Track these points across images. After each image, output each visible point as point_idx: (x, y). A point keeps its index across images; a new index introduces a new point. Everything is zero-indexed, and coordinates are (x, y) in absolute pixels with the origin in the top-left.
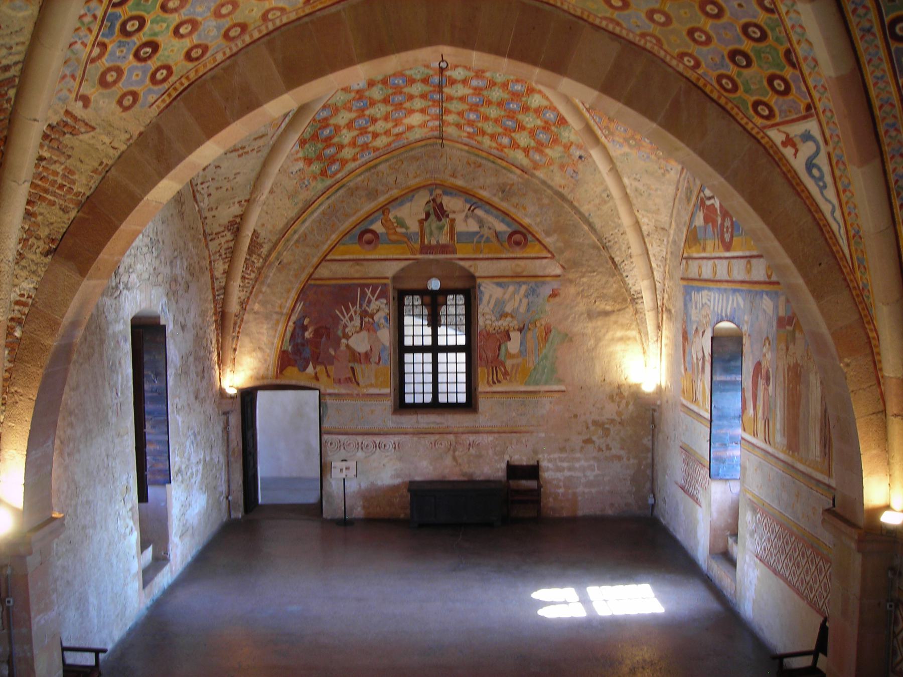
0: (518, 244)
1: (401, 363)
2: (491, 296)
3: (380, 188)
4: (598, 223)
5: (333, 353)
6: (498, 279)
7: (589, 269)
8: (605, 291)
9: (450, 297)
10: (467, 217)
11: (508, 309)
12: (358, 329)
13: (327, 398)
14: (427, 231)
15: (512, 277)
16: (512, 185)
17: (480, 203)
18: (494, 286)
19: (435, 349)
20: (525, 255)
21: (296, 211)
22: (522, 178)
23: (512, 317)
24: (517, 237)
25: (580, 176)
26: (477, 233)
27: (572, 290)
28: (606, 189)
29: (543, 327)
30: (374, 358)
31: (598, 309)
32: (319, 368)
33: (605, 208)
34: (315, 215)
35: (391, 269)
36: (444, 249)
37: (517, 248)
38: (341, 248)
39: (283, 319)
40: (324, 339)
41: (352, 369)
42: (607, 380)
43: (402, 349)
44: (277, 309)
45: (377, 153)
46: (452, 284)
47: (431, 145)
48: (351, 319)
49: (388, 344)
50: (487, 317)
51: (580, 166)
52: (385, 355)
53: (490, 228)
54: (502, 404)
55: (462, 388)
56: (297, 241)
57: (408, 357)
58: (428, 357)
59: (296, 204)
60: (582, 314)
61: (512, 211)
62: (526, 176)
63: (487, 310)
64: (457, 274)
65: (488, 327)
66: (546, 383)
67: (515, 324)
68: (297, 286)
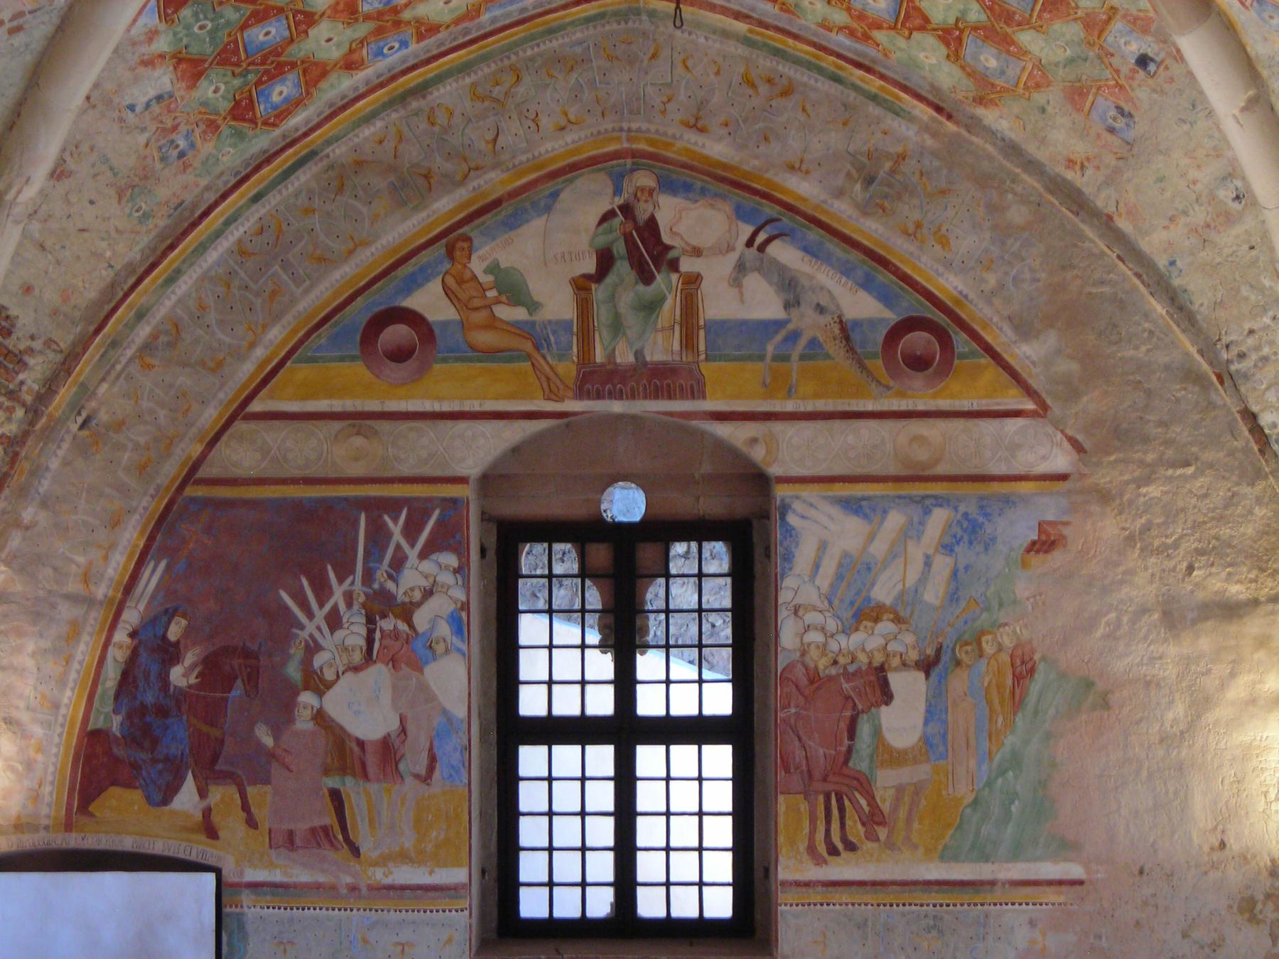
0: (918, 363)
1: (506, 780)
2: (823, 546)
3: (439, 163)
4: (1200, 291)
5: (268, 741)
6: (851, 488)
7: (1170, 453)
8: (1225, 532)
9: (679, 548)
10: (741, 268)
11: (883, 593)
12: (357, 657)
13: (246, 898)
14: (602, 315)
15: (898, 479)
16: (902, 157)
17: (787, 221)
18: (835, 511)
19: (625, 730)
20: (944, 404)
21: (144, 240)
22: (934, 135)
23: (898, 620)
24: (919, 340)
25: (1141, 127)
26: (778, 324)
27: (1109, 527)
28: (1233, 173)
29: (1005, 657)
30: (413, 762)
31: (1200, 595)
32: (217, 794)
33: (1229, 238)
34: (212, 256)
35: (476, 450)
36: (660, 380)
37: (917, 380)
38: (299, 372)
39: (95, 618)
40: (237, 691)
41: (336, 796)
42: (1234, 845)
43: (512, 731)
44: (73, 587)
46: (685, 505)
48: (334, 621)
49: (460, 712)
50: (811, 618)
51: (1142, 93)
52: (450, 752)
53: (821, 309)
54: (862, 926)
55: (721, 867)
56: (148, 347)
57: (531, 758)
58: (602, 757)
59: (146, 216)
60: (1144, 611)
61: (900, 249)
62: (951, 127)
63: (809, 595)
64: (706, 468)
65: (814, 653)
66: (1016, 854)
67: (906, 644)
68: (145, 506)
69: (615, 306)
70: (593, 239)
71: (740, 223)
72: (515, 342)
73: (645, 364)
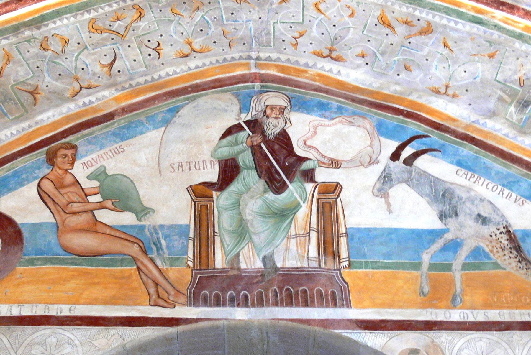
3: (48, 82)
10: (386, 178)
14: (224, 221)
36: (293, 286)
53: (483, 220)
69: (240, 214)
70: (215, 151)
71: (382, 139)
72: (117, 246)
73: (277, 269)
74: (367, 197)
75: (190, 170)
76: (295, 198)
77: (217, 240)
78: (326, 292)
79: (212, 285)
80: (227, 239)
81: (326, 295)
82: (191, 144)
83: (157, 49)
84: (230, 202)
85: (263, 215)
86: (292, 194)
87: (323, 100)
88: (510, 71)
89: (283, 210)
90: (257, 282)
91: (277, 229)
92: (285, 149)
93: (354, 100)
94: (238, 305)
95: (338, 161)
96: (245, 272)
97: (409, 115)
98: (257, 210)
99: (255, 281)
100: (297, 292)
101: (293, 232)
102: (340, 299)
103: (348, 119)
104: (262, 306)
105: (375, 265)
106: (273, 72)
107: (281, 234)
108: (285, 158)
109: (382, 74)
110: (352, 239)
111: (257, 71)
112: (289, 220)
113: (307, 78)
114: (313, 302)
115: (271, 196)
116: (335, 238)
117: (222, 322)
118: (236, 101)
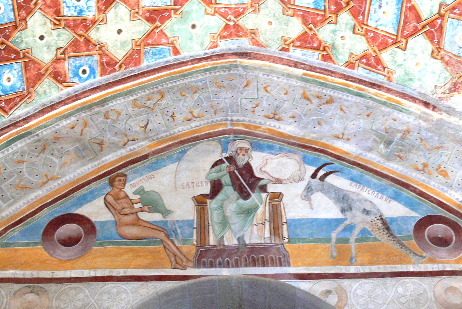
3: (109, 137)
10: (309, 189)
14: (214, 216)
16: (408, 132)
17: (337, 164)
22: (426, 120)
26: (338, 222)
36: (256, 255)
37: (443, 252)
45: (110, 77)
47: (224, 68)
53: (367, 212)
62: (435, 115)
69: (223, 212)
70: (208, 175)
71: (306, 166)
72: (151, 233)
73: (246, 245)
74: (298, 200)
75: (193, 187)
76: (256, 203)
77: (211, 228)
78: (276, 257)
79: (208, 255)
80: (216, 228)
81: (276, 259)
82: (194, 172)
83: (173, 116)
84: (217, 206)
85: (238, 213)
86: (254, 200)
87: (271, 144)
88: (380, 123)
89: (249, 210)
90: (234, 253)
91: (246, 221)
92: (248, 173)
93: (289, 143)
94: (224, 267)
95: (280, 180)
96: (227, 247)
97: (322, 151)
98: (233, 210)
99: (233, 252)
100: (258, 259)
101: (255, 223)
102: (284, 262)
103: (286, 155)
104: (238, 267)
105: (304, 241)
106: (241, 128)
107: (248, 224)
108: (249, 178)
109: (305, 128)
110: (290, 226)
111: (231, 128)
112: (252, 215)
113: (261, 131)
114: (268, 264)
115: (241, 201)
116: (280, 225)
117: (214, 277)
118: (219, 146)
